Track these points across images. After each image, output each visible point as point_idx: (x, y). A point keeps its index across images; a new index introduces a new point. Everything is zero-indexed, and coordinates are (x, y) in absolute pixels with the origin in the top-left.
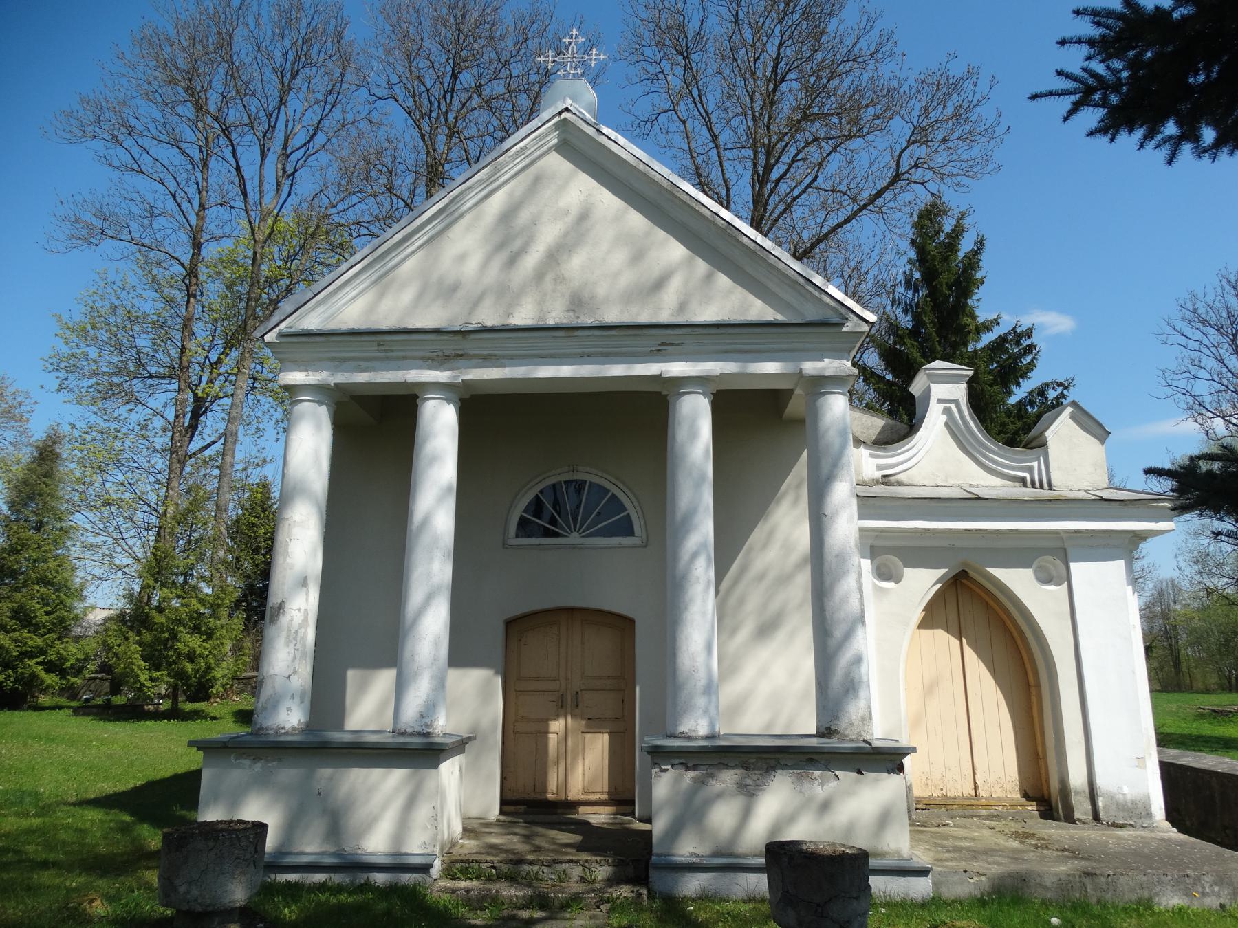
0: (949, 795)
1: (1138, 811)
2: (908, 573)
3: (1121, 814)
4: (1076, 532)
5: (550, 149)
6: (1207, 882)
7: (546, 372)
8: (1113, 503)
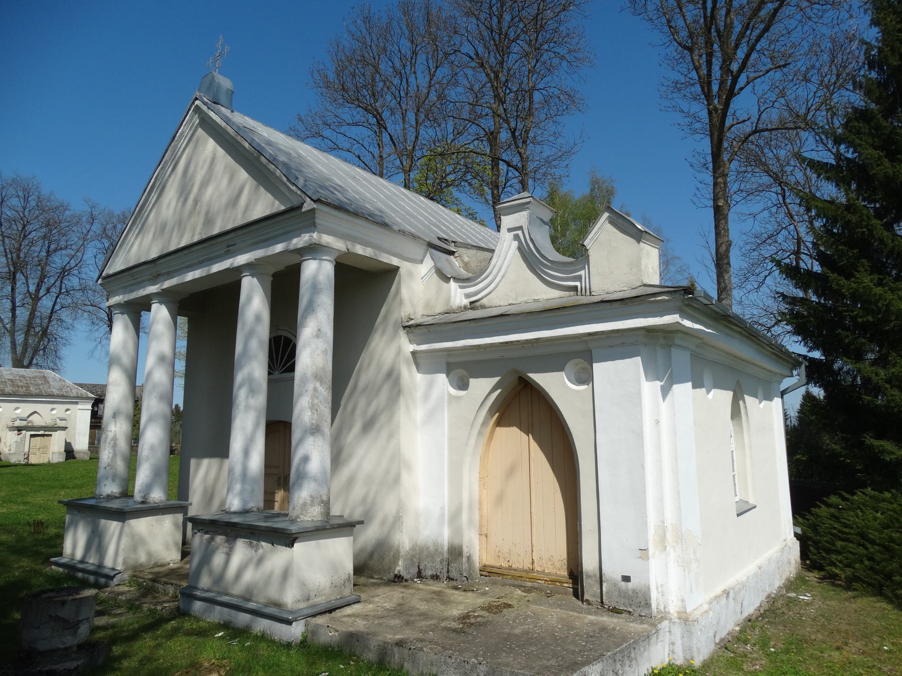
0: (513, 566)
1: (638, 600)
2: (472, 381)
3: (623, 601)
4: (590, 334)
5: (196, 127)
6: (482, 672)
7: (190, 276)
8: (614, 303)
